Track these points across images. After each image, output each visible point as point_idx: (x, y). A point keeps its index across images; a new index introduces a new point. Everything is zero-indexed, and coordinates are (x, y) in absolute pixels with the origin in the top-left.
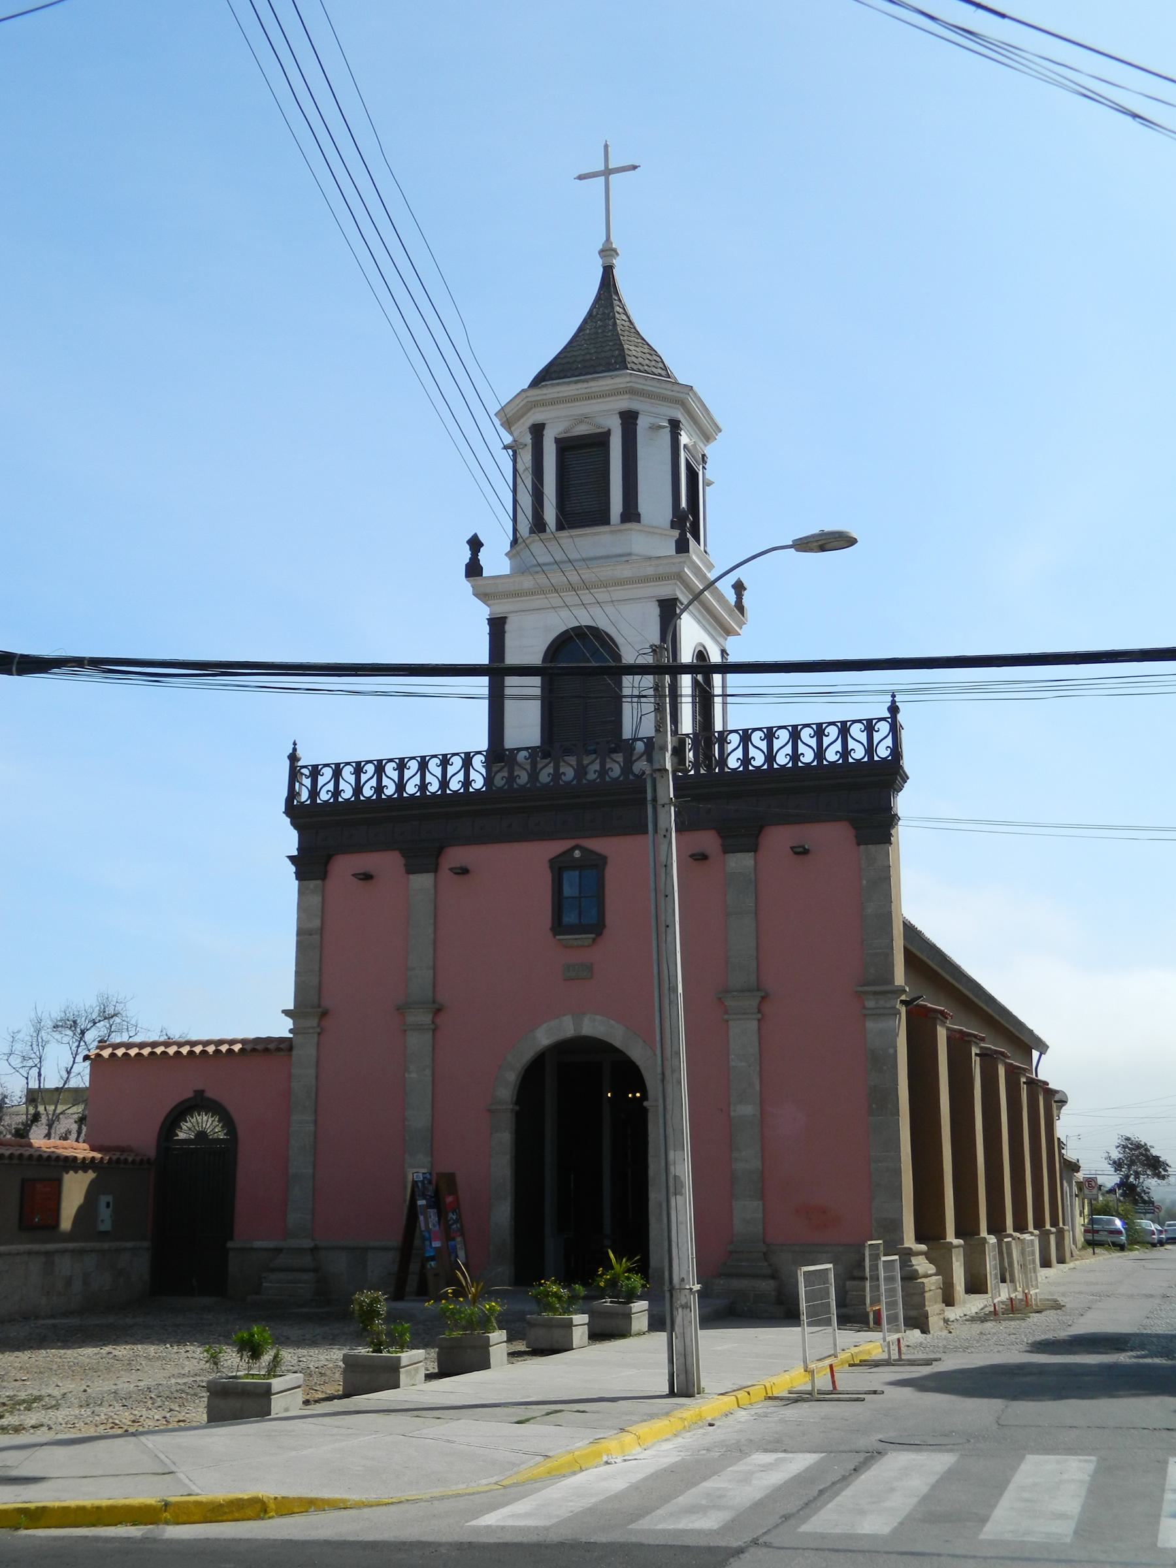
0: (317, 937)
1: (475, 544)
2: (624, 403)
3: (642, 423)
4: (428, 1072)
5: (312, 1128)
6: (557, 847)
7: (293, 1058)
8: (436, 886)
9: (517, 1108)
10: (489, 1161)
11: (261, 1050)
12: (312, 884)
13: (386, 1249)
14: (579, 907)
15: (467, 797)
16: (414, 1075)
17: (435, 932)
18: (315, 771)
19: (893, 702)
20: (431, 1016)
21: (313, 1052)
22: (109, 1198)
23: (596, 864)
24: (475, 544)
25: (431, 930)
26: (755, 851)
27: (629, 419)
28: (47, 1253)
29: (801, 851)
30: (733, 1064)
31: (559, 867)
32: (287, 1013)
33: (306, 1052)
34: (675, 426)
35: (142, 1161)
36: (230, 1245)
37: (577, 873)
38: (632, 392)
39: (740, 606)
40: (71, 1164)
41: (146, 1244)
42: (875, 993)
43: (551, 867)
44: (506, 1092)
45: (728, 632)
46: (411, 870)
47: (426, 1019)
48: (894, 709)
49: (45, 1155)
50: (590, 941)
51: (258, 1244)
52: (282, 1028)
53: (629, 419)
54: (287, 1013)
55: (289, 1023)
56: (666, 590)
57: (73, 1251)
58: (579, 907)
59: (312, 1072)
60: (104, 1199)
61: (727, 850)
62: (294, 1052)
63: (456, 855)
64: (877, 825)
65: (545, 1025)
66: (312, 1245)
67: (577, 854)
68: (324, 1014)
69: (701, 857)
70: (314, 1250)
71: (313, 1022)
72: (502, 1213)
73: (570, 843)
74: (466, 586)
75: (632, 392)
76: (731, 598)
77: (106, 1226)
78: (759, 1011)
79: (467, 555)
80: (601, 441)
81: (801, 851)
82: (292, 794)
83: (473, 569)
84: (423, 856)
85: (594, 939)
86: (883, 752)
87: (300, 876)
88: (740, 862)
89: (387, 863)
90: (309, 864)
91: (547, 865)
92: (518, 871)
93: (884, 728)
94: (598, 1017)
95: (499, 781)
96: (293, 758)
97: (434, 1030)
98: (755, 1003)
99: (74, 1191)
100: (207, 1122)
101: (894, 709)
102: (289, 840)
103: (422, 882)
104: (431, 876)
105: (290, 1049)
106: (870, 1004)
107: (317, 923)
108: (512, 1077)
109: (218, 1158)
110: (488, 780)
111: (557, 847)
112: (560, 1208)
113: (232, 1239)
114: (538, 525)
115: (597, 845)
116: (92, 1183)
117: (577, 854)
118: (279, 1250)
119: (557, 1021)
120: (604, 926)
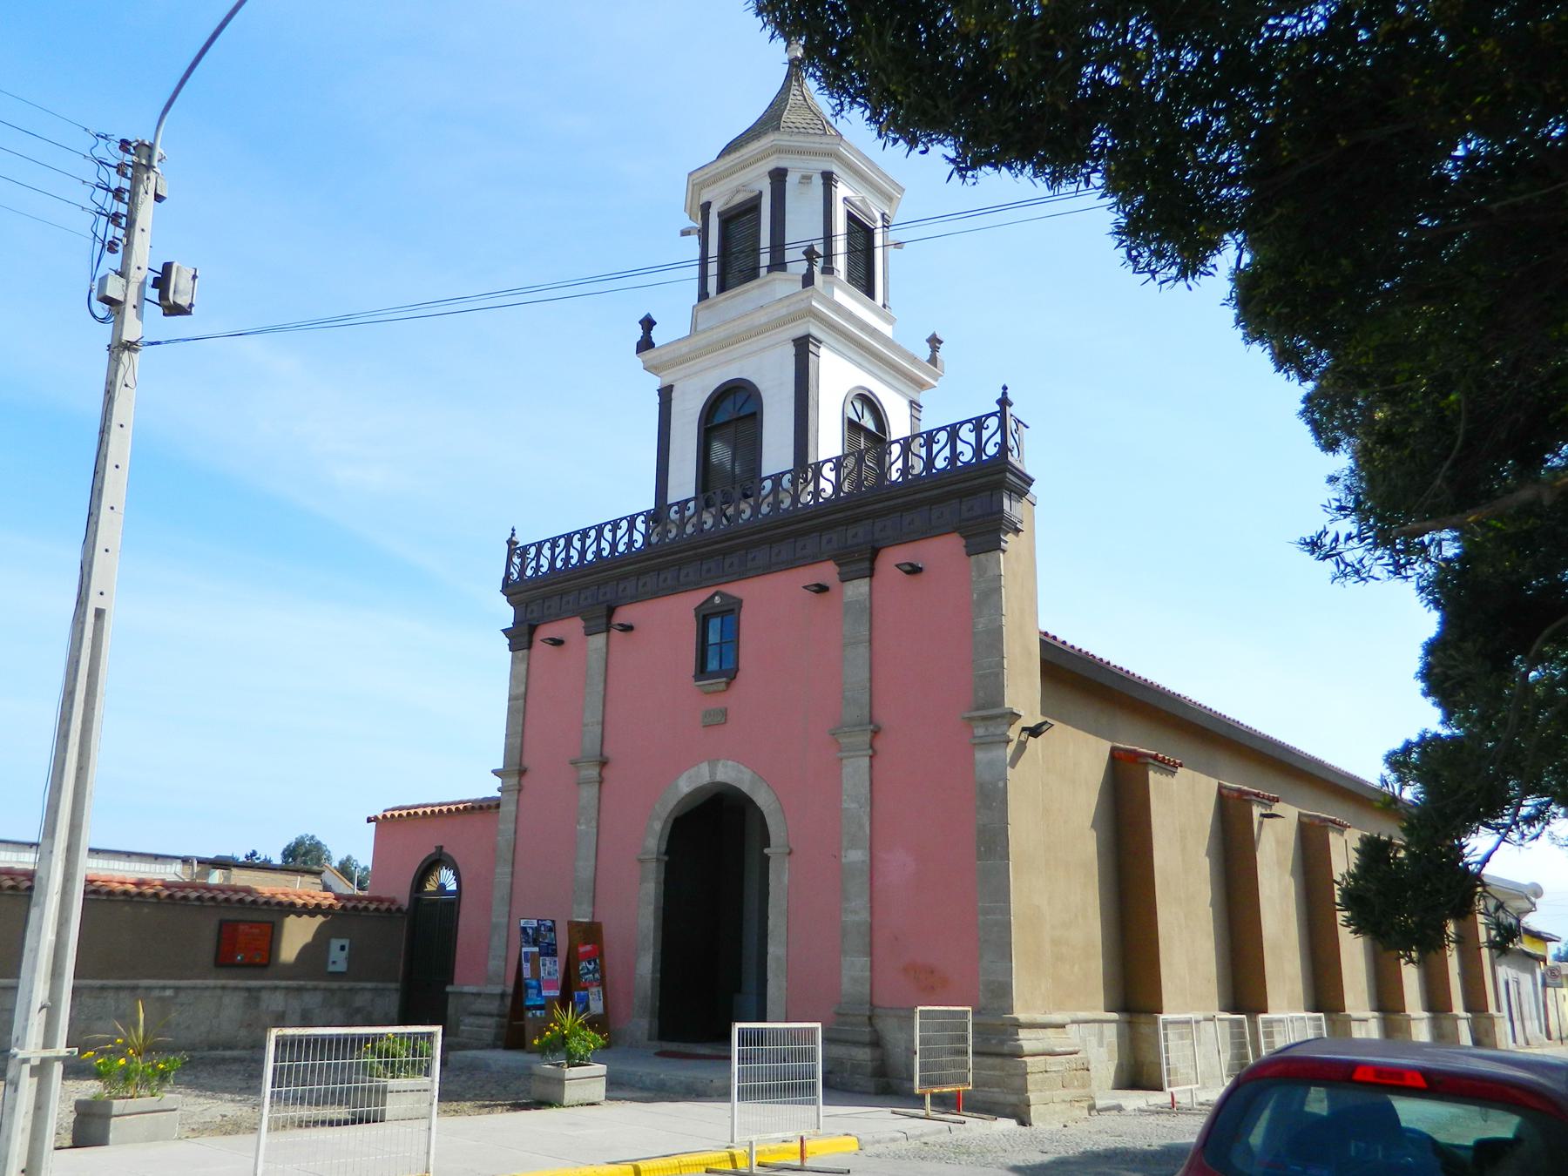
0: (521, 702)
1: (648, 323)
2: (773, 163)
3: (792, 180)
4: (594, 824)
5: (509, 880)
6: (700, 596)
10: (634, 916)
11: (483, 808)
12: (520, 654)
15: (631, 557)
17: (605, 688)
18: (525, 549)
19: (1004, 393)
22: (346, 942)
23: (731, 611)
24: (648, 323)
26: (871, 576)
27: (778, 177)
28: (249, 989)
29: (914, 570)
30: (845, 805)
31: (704, 618)
32: (496, 772)
33: (508, 809)
34: (828, 179)
35: (254, 902)
36: (449, 989)
38: (780, 150)
39: (933, 360)
40: (290, 909)
41: (393, 986)
42: (984, 718)
45: (921, 385)
46: (588, 633)
47: (593, 772)
48: (1004, 402)
49: (262, 900)
50: (723, 686)
51: (466, 989)
52: (490, 788)
53: (778, 177)
54: (496, 772)
55: (498, 782)
56: (799, 331)
57: (287, 988)
59: (512, 826)
60: (335, 944)
61: (844, 579)
65: (686, 775)
68: (522, 772)
71: (514, 781)
72: (646, 966)
74: (638, 361)
75: (780, 150)
76: (924, 352)
77: (341, 967)
78: (871, 747)
79: (638, 333)
80: (752, 206)
81: (914, 570)
82: (508, 574)
83: (645, 344)
84: (603, 619)
85: (728, 684)
86: (991, 450)
87: (512, 648)
88: (858, 589)
90: (521, 637)
92: (667, 621)
93: (993, 423)
95: (654, 539)
96: (511, 542)
97: (601, 783)
98: (867, 738)
99: (296, 936)
100: (447, 878)
101: (1004, 402)
102: (506, 614)
103: (599, 640)
105: (498, 806)
106: (980, 731)
109: (449, 907)
110: (646, 536)
111: (700, 596)
112: (697, 966)
113: (452, 983)
114: (703, 295)
115: (733, 589)
116: (322, 926)
117: (717, 600)
120: (737, 670)
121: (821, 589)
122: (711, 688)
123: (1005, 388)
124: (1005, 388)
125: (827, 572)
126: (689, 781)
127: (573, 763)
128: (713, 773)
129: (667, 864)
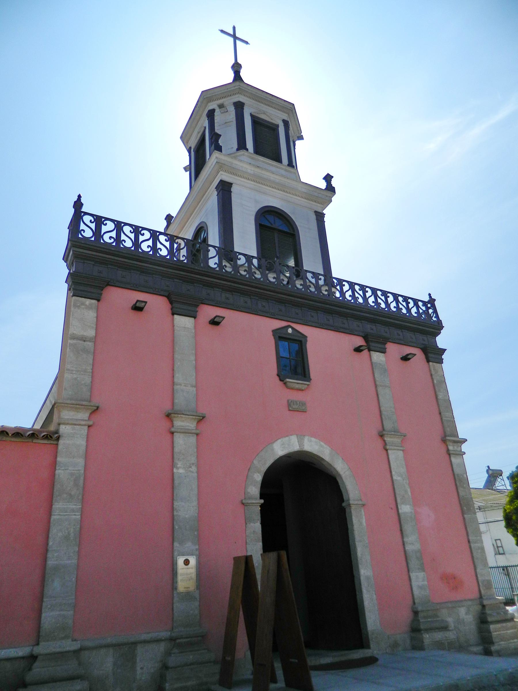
4: (194, 469)
6: (278, 324)
7: (60, 447)
8: (195, 327)
9: (262, 501)
13: (158, 641)
14: (294, 365)
16: (181, 471)
20: (195, 424)
21: (84, 443)
25: (193, 358)
37: (286, 343)
43: (274, 335)
44: (255, 490)
47: (191, 424)
58: (294, 365)
59: (81, 461)
62: (61, 442)
63: (208, 312)
64: (434, 355)
65: (279, 441)
66: (76, 646)
67: (290, 331)
69: (358, 350)
70: (77, 652)
73: (284, 324)
84: (183, 304)
88: (377, 357)
89: (157, 304)
91: (272, 333)
94: (313, 439)
103: (183, 322)
104: (192, 320)
107: (92, 333)
108: (259, 478)
111: (278, 324)
117: (290, 331)
118: (33, 658)
119: (287, 438)
121: (358, 350)
122: (297, 386)
123: (430, 295)
124: (430, 295)
125: (359, 341)
126: (281, 448)
127: (168, 416)
128: (301, 444)
129: (262, 506)
